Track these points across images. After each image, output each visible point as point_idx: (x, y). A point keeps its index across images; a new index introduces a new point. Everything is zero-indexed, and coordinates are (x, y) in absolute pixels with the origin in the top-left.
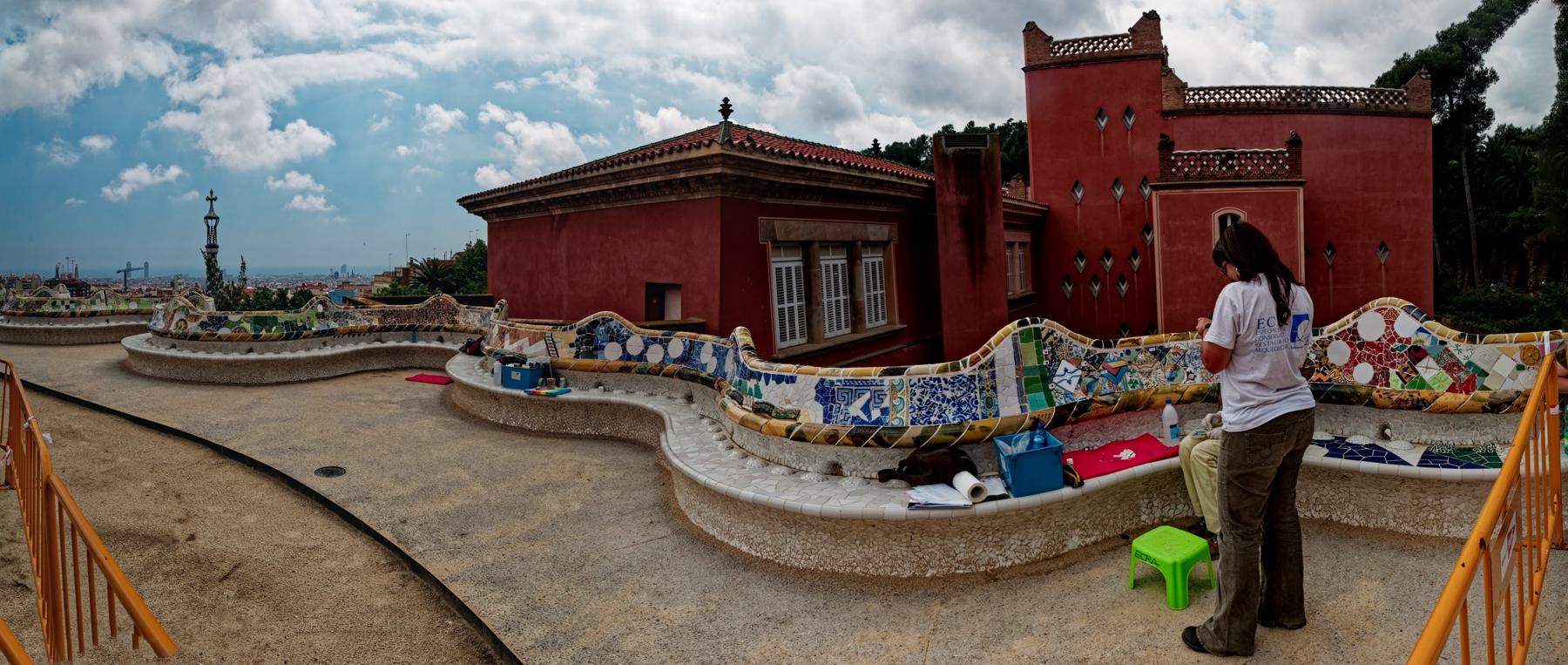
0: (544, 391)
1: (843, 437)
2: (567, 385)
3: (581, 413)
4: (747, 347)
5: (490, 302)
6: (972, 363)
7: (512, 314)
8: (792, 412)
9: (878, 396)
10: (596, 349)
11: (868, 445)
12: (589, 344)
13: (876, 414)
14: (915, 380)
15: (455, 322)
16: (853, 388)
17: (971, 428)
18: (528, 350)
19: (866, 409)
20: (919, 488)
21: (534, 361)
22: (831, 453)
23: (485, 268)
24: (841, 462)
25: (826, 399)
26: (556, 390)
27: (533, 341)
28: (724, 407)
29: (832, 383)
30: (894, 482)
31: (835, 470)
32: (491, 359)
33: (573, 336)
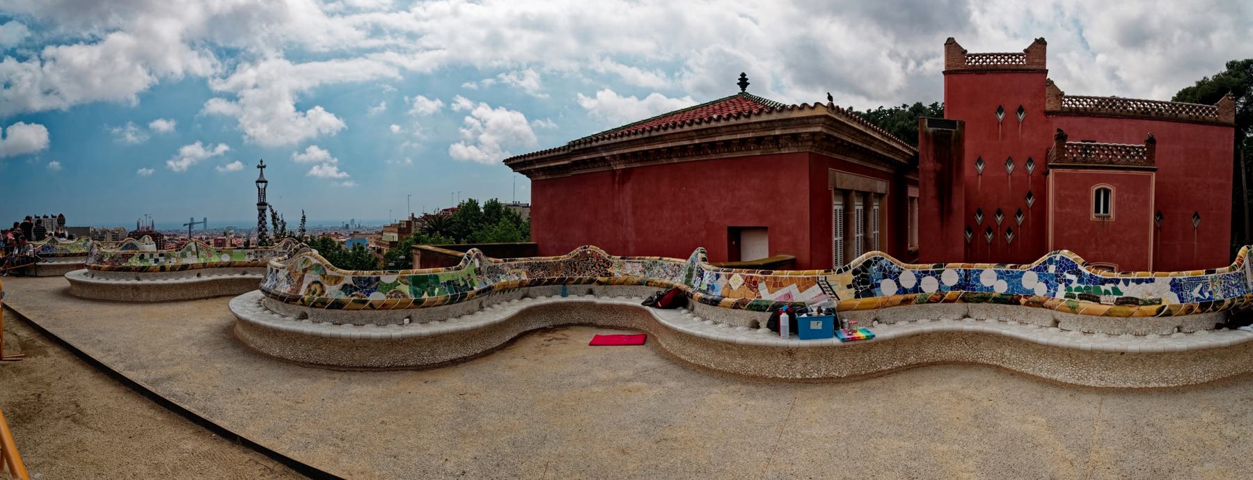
10: (872, 287)
12: (865, 283)
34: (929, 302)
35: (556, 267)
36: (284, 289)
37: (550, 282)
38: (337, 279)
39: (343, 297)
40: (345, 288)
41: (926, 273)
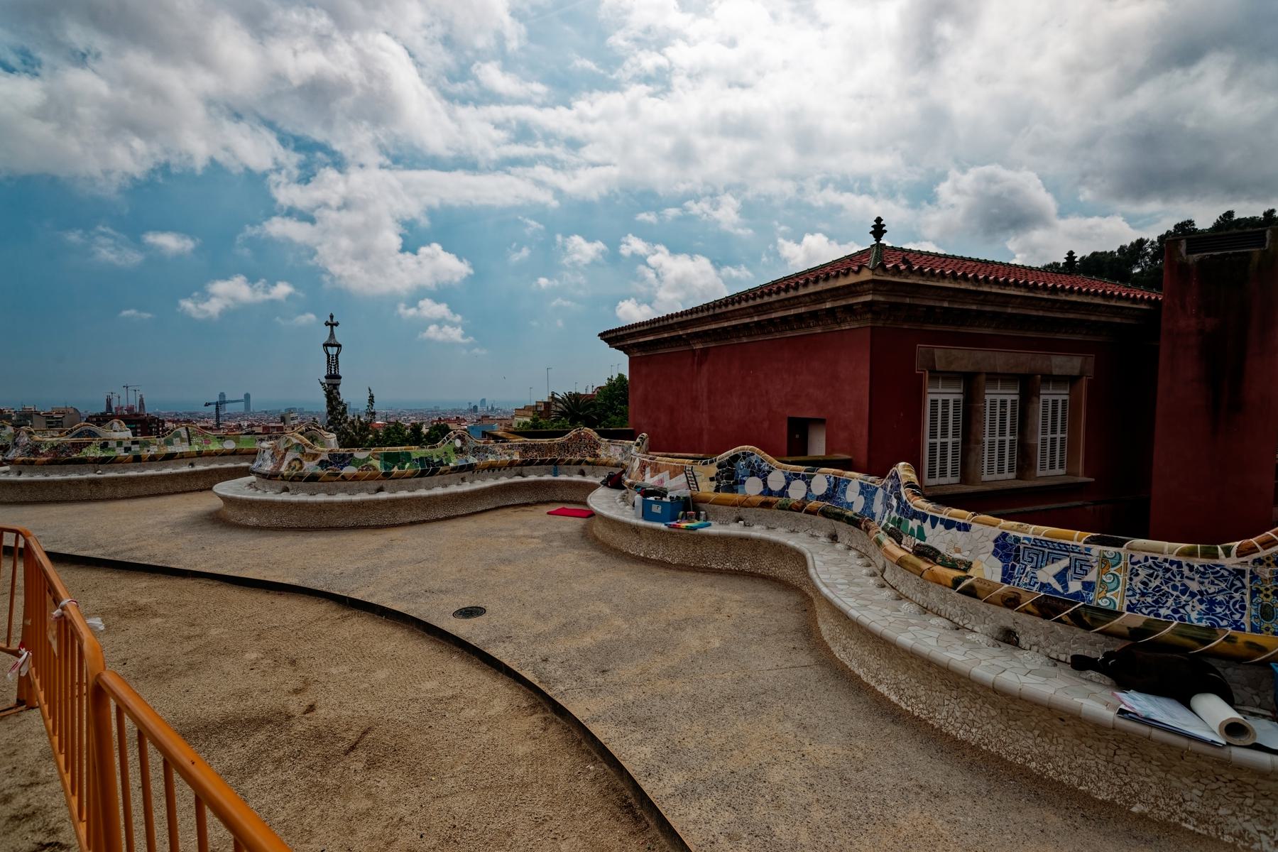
0: (684, 525)
1: (1026, 602)
2: (707, 518)
3: (721, 548)
4: (910, 485)
5: (631, 436)
6: (1241, 553)
7: (653, 447)
8: (962, 562)
9: (1081, 566)
11: (1060, 620)
13: (1074, 586)
14: (1139, 556)
15: (597, 456)
16: (1045, 552)
17: (1229, 639)
18: (668, 484)
19: (1061, 577)
20: (1132, 693)
21: (674, 494)
22: (1007, 617)
23: (626, 403)
24: (1018, 629)
25: (1008, 556)
26: (696, 523)
27: (674, 474)
28: (879, 543)
29: (1017, 540)
30: (1093, 674)
31: (1008, 638)
32: (632, 492)
33: (713, 470)
34: (790, 509)
35: (550, 448)
36: (268, 467)
37: (542, 462)
38: (315, 456)
39: (319, 471)
40: (322, 463)
41: (797, 476)
